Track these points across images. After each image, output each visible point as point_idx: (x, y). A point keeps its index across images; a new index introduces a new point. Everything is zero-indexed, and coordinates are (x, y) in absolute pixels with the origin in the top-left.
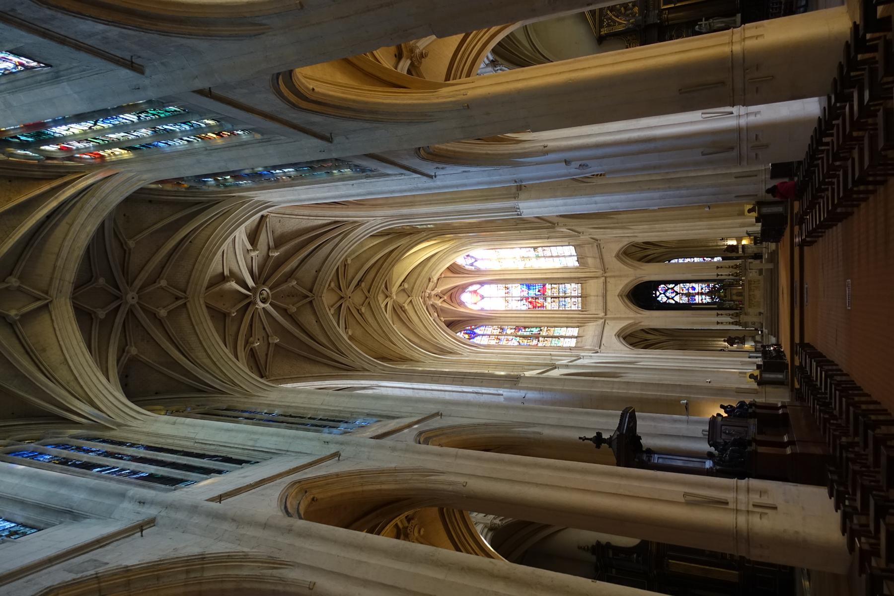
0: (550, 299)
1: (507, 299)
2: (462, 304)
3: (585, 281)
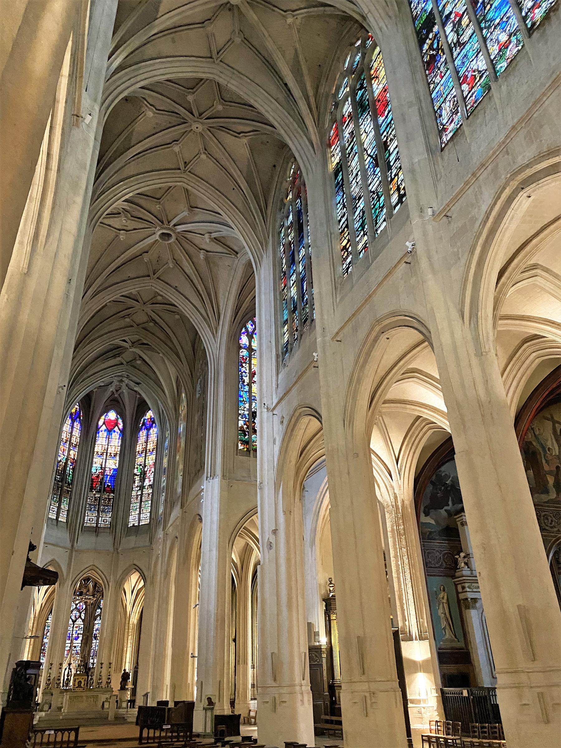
0: (99, 495)
1: (105, 454)
2: (106, 411)
3: (112, 532)
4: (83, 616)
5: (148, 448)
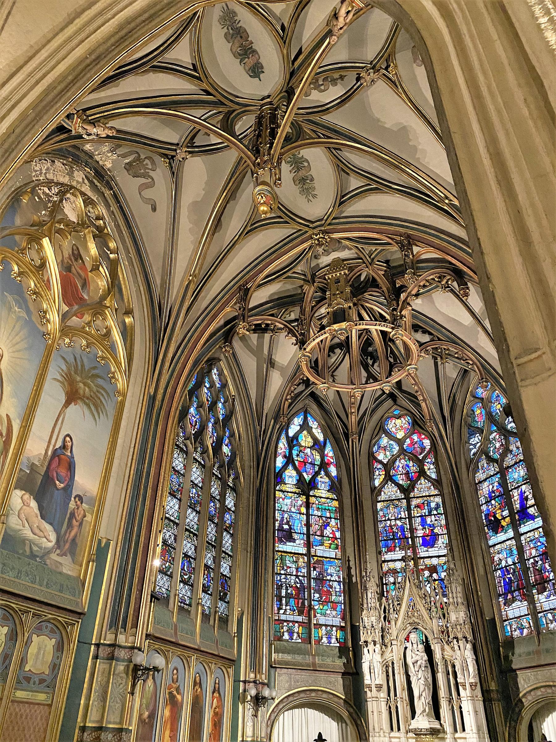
4: (431, 470)
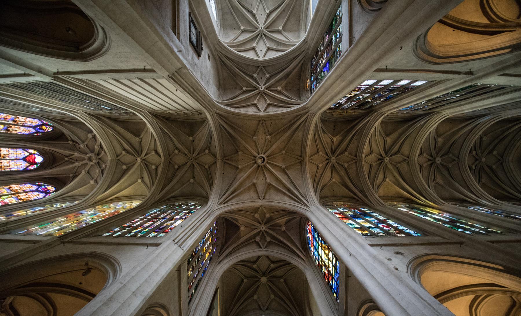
5: (19, 195)
